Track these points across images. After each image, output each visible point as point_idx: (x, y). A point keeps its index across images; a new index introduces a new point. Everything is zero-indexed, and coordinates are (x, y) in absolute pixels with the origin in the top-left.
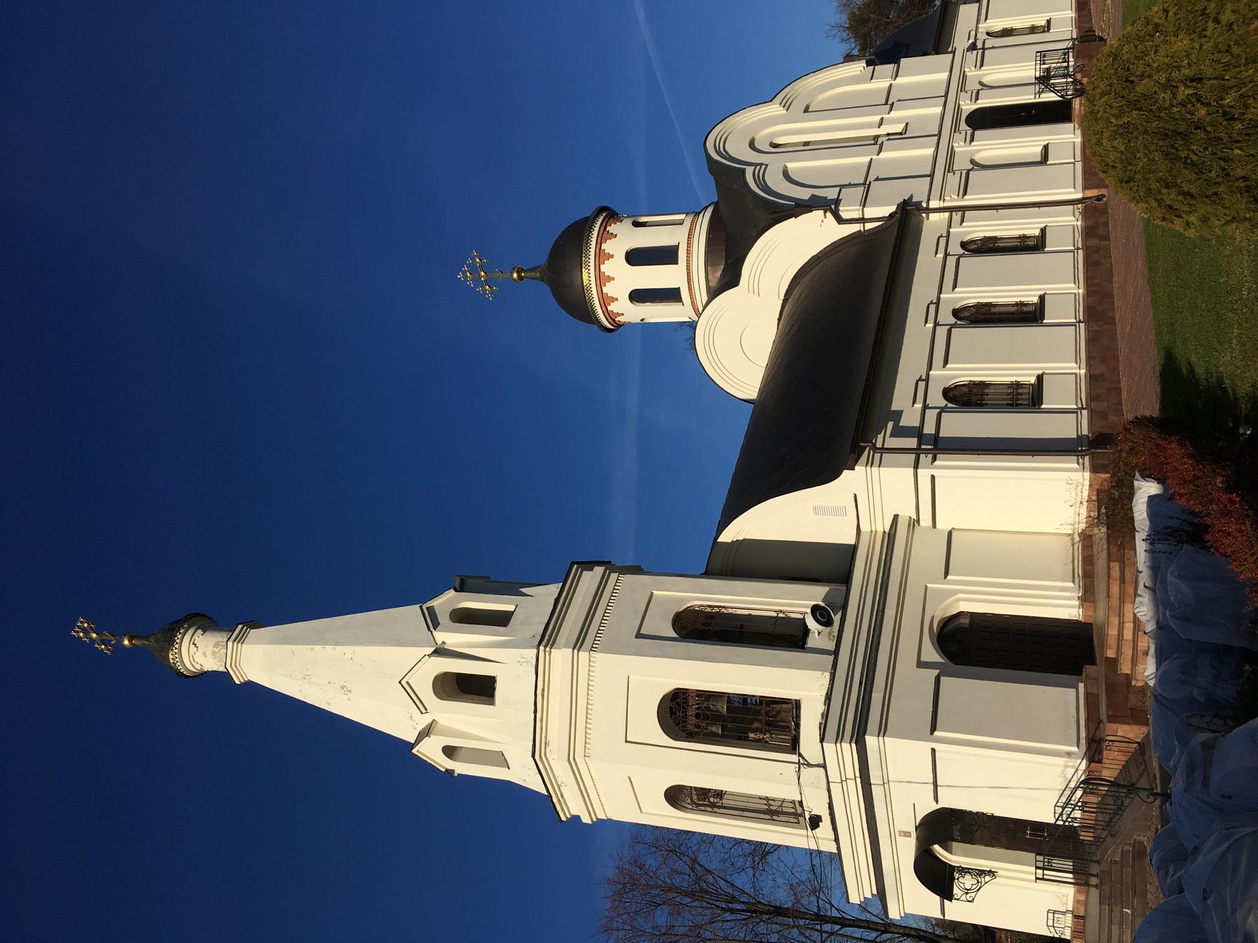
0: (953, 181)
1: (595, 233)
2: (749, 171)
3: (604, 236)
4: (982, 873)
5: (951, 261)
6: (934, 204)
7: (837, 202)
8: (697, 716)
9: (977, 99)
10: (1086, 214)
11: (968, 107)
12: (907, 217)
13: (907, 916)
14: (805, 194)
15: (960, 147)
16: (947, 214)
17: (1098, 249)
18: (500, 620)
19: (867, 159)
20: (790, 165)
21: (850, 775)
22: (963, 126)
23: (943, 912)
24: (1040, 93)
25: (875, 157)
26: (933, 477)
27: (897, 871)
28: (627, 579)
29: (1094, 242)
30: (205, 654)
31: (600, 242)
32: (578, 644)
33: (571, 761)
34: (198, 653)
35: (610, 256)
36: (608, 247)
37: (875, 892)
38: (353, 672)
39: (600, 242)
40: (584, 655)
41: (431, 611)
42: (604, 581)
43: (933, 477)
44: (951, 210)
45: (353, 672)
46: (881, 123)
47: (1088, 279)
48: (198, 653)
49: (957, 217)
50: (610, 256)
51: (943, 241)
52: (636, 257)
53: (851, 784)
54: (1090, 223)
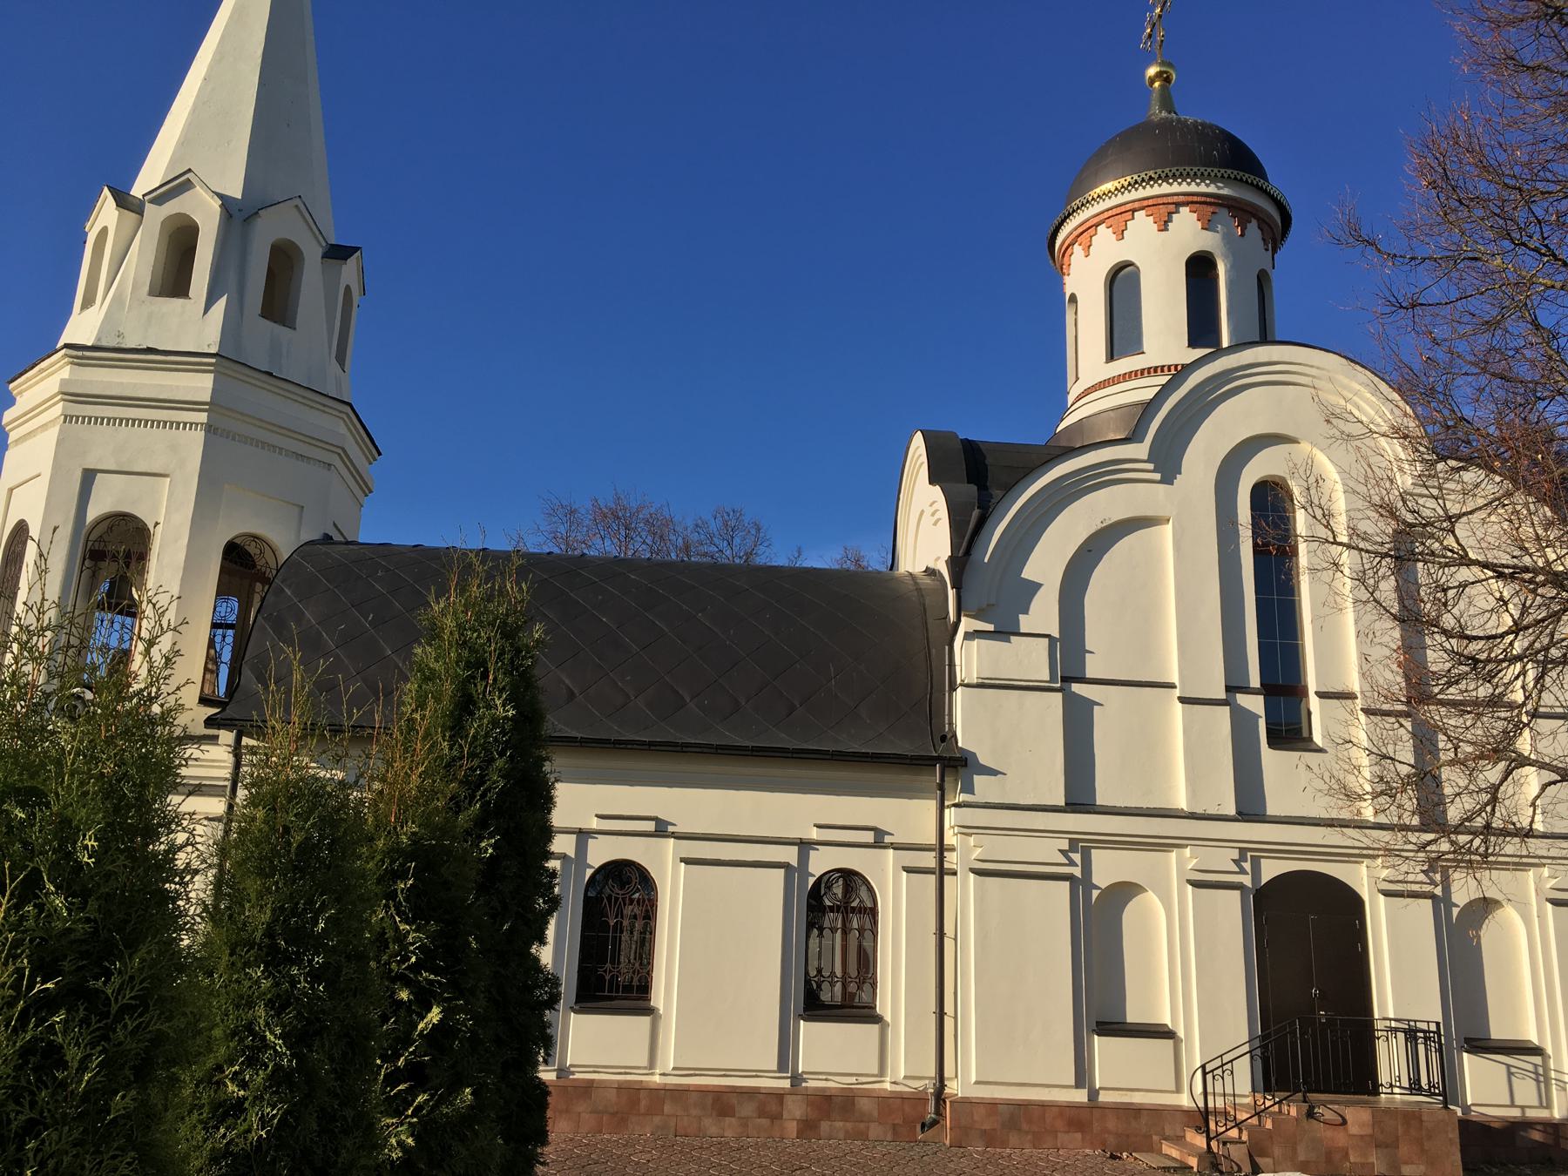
0: (1048, 852)
1: (1165, 188)
2: (1140, 450)
3: (1164, 211)
5: (790, 855)
6: (950, 815)
7: (1005, 632)
9: (1387, 894)
10: (918, 1099)
11: (1362, 878)
12: (944, 766)
14: (1046, 563)
15: (1177, 864)
16: (932, 840)
17: (776, 1117)
18: (173, 280)
19: (1175, 679)
20: (1167, 530)
22: (1271, 869)
24: (1411, 1034)
25: (1177, 693)
28: (199, 436)
29: (795, 1110)
31: (1147, 205)
32: (72, 396)
35: (1120, 235)
36: (1142, 223)
39: (1147, 205)
40: (58, 410)
41: (187, 186)
42: (193, 405)
44: (941, 849)
46: (1321, 695)
47: (678, 1094)
49: (929, 860)
50: (1120, 235)
51: (869, 837)
52: (1122, 283)
54: (865, 1105)
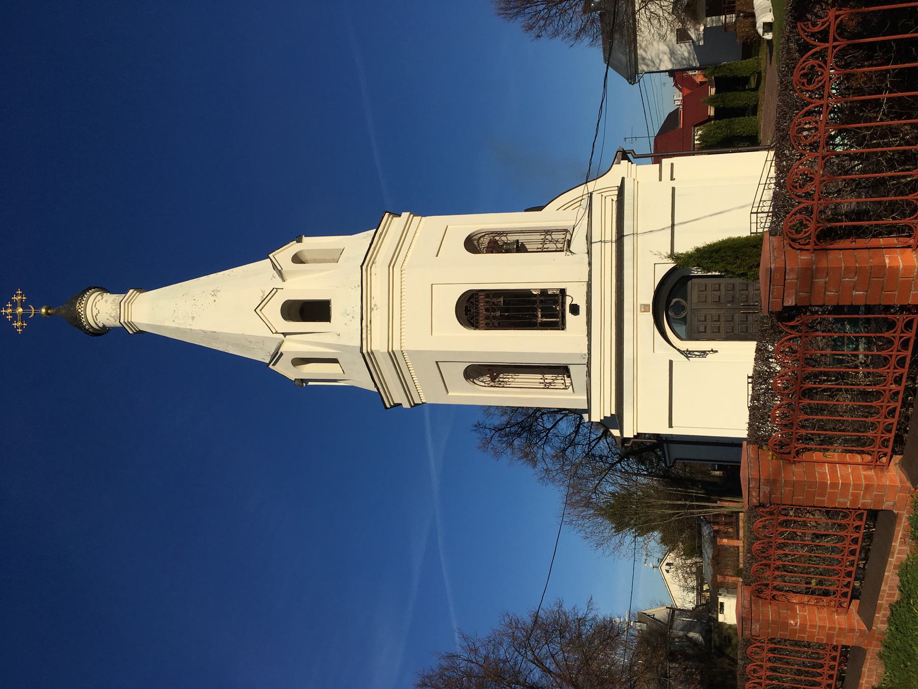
4: (704, 353)
8: (487, 310)
13: (639, 435)
21: (608, 238)
23: (671, 426)
26: (672, 164)
27: (635, 361)
30: (106, 301)
33: (391, 265)
34: (100, 309)
37: (613, 412)
38: (218, 309)
43: (672, 164)
45: (218, 309)
48: (100, 309)
53: (608, 245)
